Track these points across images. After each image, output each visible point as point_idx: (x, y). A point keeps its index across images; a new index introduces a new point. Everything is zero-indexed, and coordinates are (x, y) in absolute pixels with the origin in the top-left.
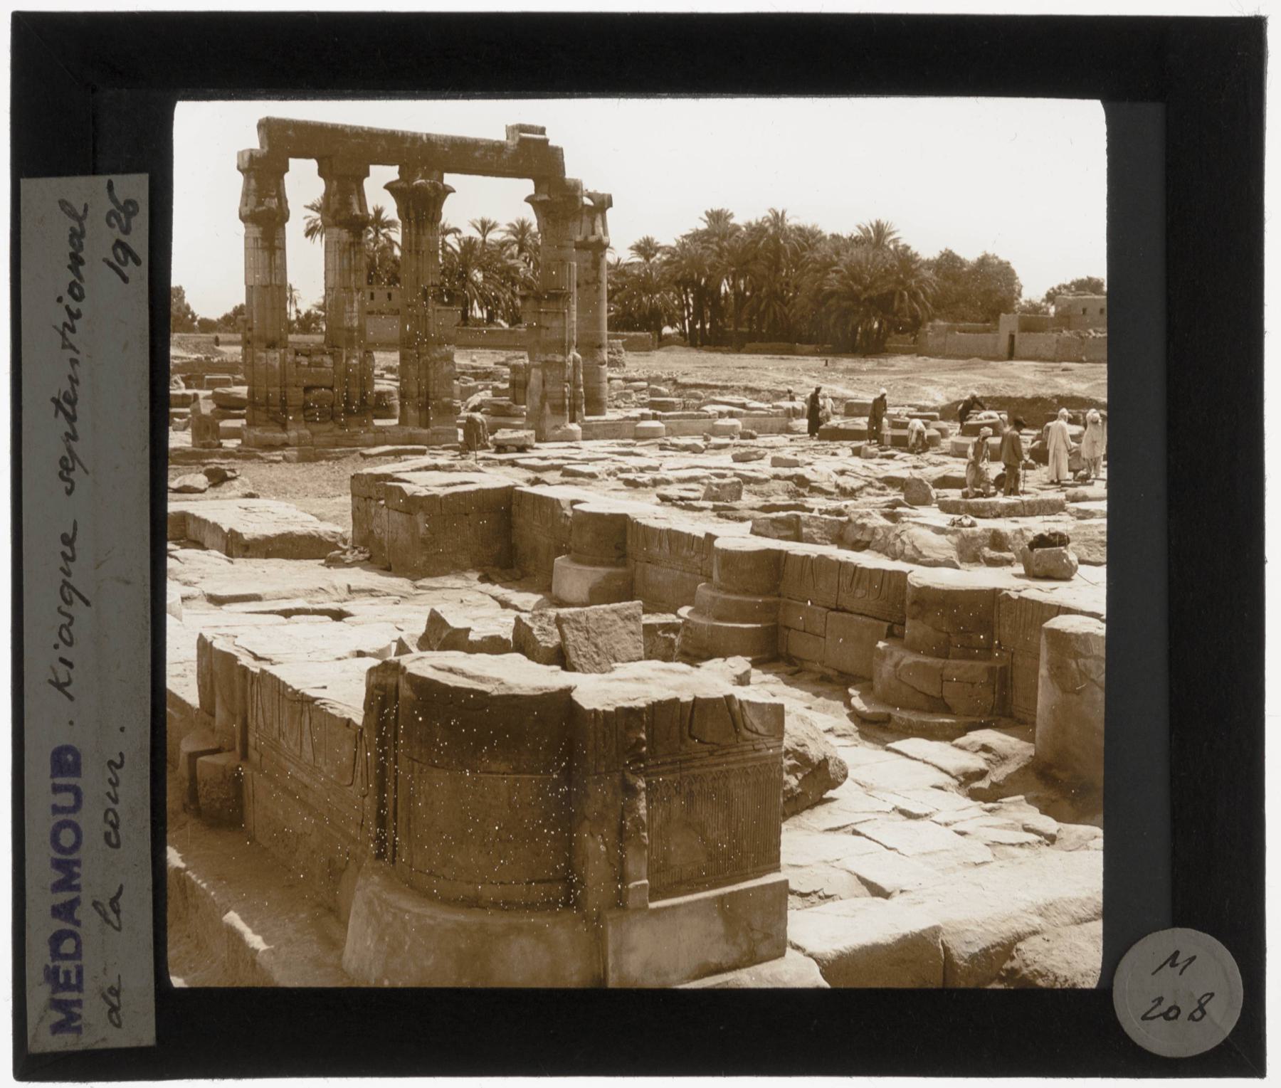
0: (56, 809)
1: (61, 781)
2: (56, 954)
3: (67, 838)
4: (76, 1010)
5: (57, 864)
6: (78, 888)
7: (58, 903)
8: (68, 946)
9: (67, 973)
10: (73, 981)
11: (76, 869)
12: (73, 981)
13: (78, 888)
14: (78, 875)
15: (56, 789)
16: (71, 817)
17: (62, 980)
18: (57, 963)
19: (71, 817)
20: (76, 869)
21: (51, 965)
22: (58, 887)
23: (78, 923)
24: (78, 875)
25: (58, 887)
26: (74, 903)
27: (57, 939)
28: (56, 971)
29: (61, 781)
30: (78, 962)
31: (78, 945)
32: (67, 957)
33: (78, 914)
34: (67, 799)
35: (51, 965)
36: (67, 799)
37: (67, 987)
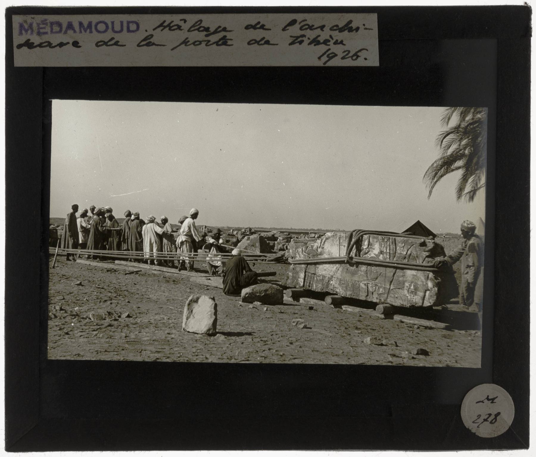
0: (113, 23)
1: (125, 25)
2: (52, 24)
3: (101, 27)
4: (29, 32)
5: (90, 24)
6: (81, 32)
7: (74, 24)
8: (56, 28)
9: (44, 28)
10: (41, 31)
11: (88, 30)
12: (41, 31)
13: (81, 32)
14: (85, 31)
15: (122, 23)
16: (110, 30)
17: (42, 26)
18: (49, 24)
19: (110, 30)
20: (88, 30)
21: (48, 21)
22: (81, 24)
23: (66, 32)
24: (85, 31)
25: (81, 24)
26: (75, 32)
27: (60, 25)
28: (46, 24)
29: (125, 25)
30: (49, 32)
31: (57, 32)
32: (52, 29)
33: (70, 32)
34: (117, 28)
35: (48, 21)
36: (117, 28)
37: (39, 28)
